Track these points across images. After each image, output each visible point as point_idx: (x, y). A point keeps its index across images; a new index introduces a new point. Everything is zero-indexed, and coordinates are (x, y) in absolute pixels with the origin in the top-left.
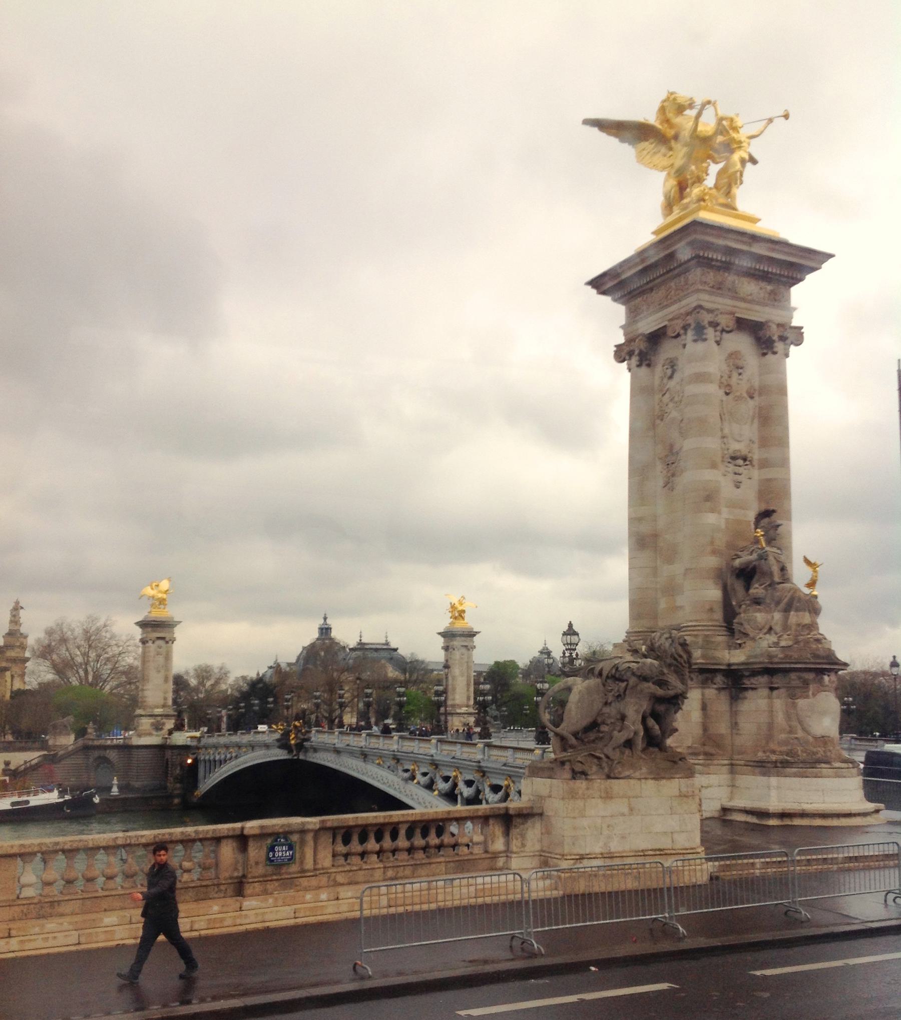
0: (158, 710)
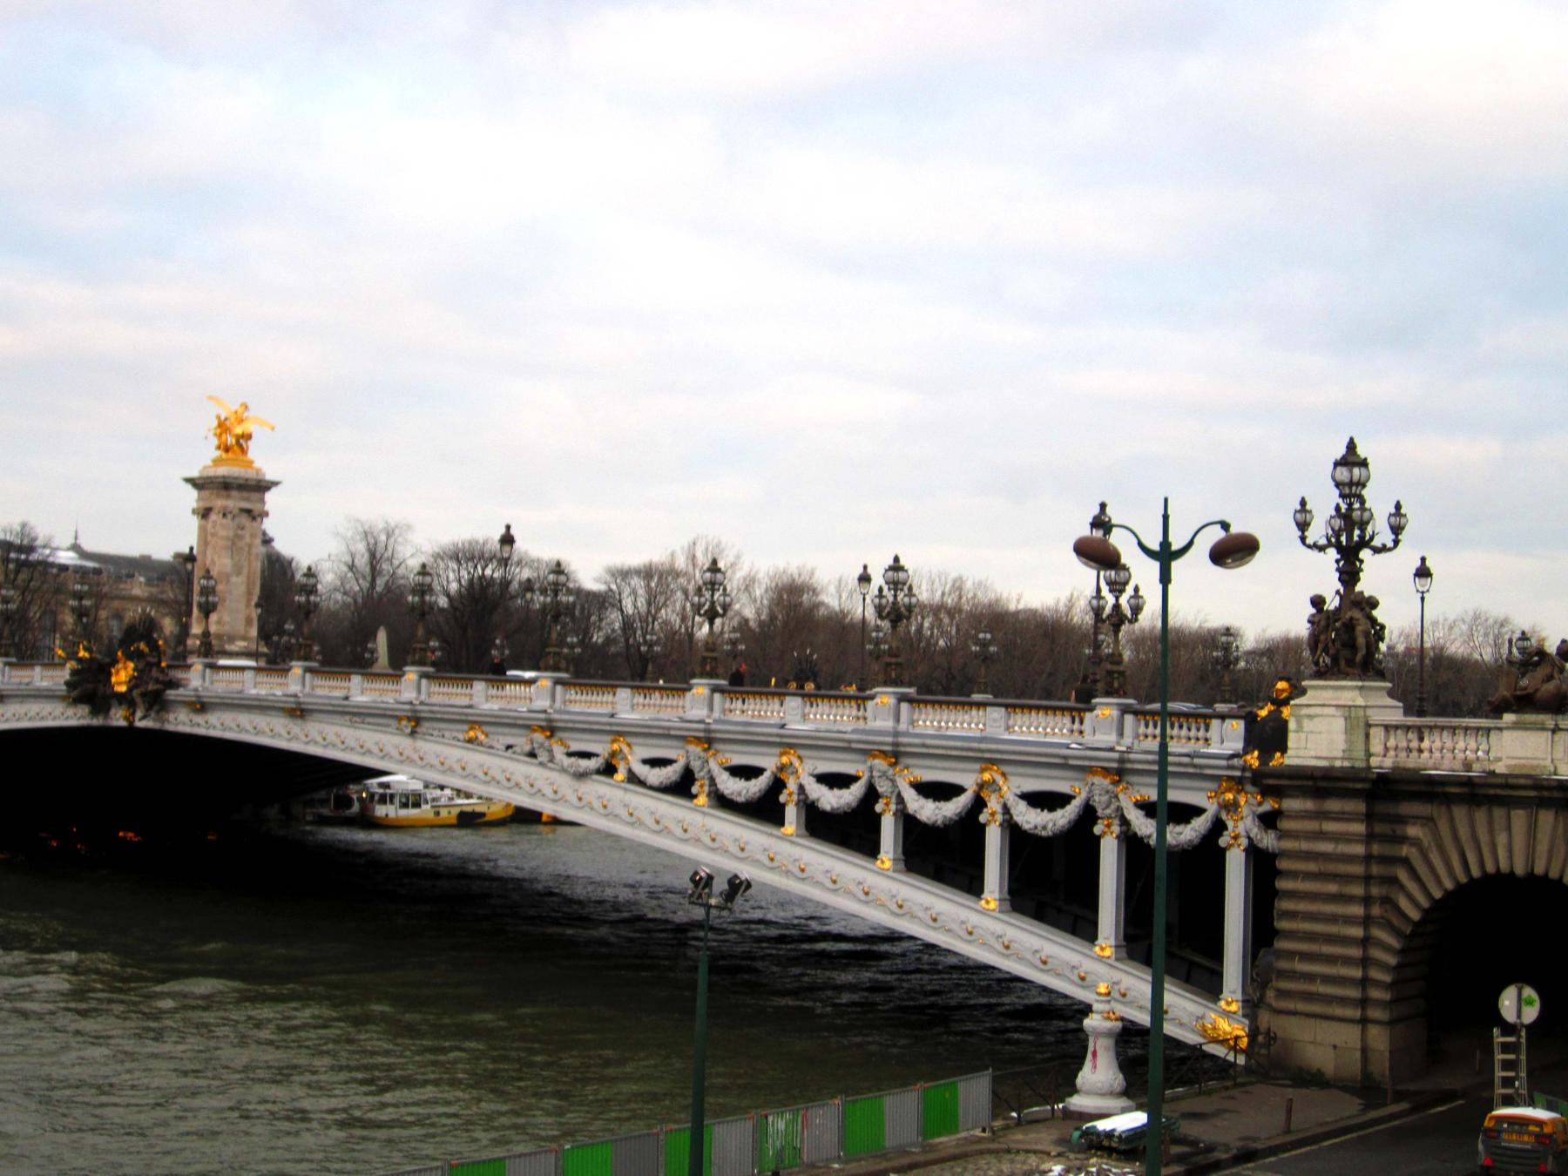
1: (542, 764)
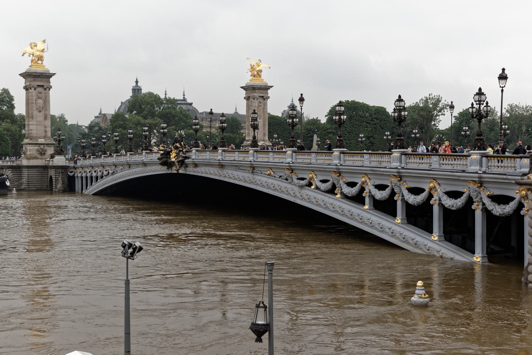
0: (41, 140)
1: (290, 183)
